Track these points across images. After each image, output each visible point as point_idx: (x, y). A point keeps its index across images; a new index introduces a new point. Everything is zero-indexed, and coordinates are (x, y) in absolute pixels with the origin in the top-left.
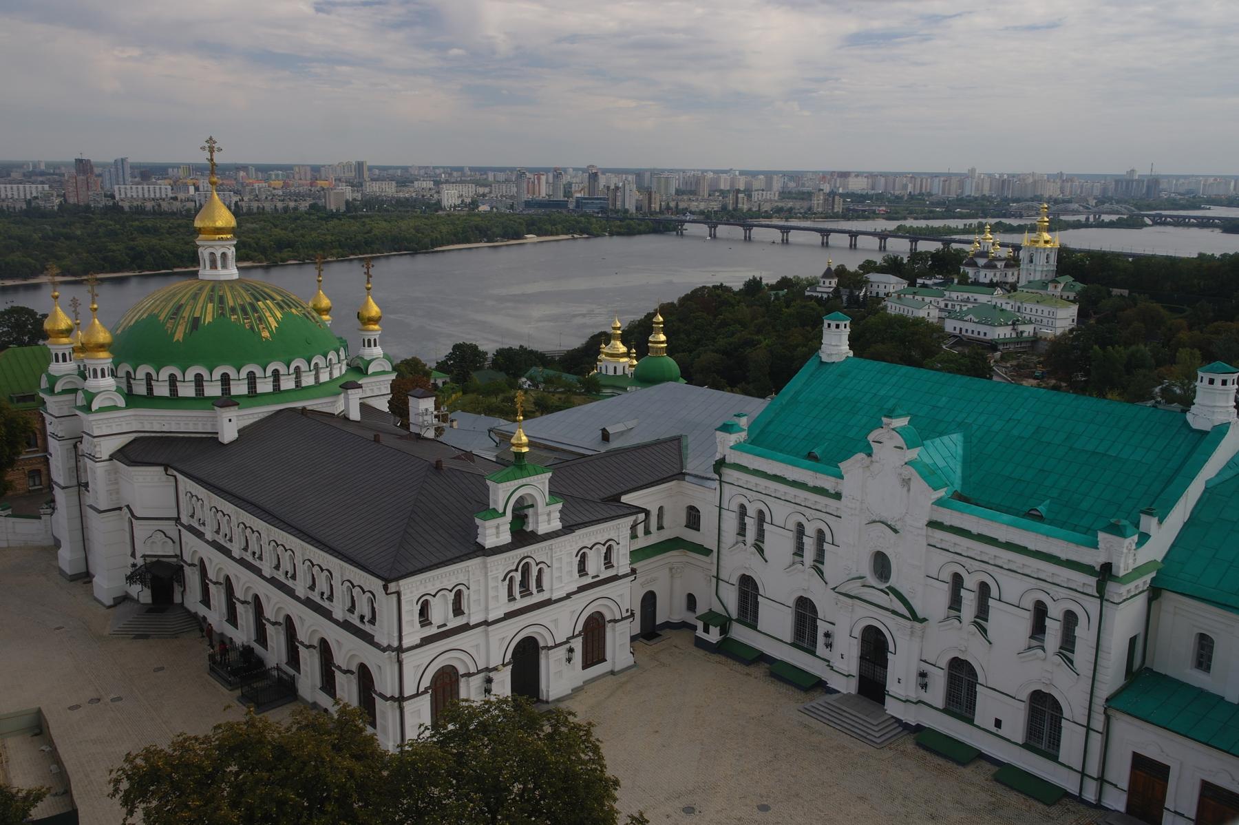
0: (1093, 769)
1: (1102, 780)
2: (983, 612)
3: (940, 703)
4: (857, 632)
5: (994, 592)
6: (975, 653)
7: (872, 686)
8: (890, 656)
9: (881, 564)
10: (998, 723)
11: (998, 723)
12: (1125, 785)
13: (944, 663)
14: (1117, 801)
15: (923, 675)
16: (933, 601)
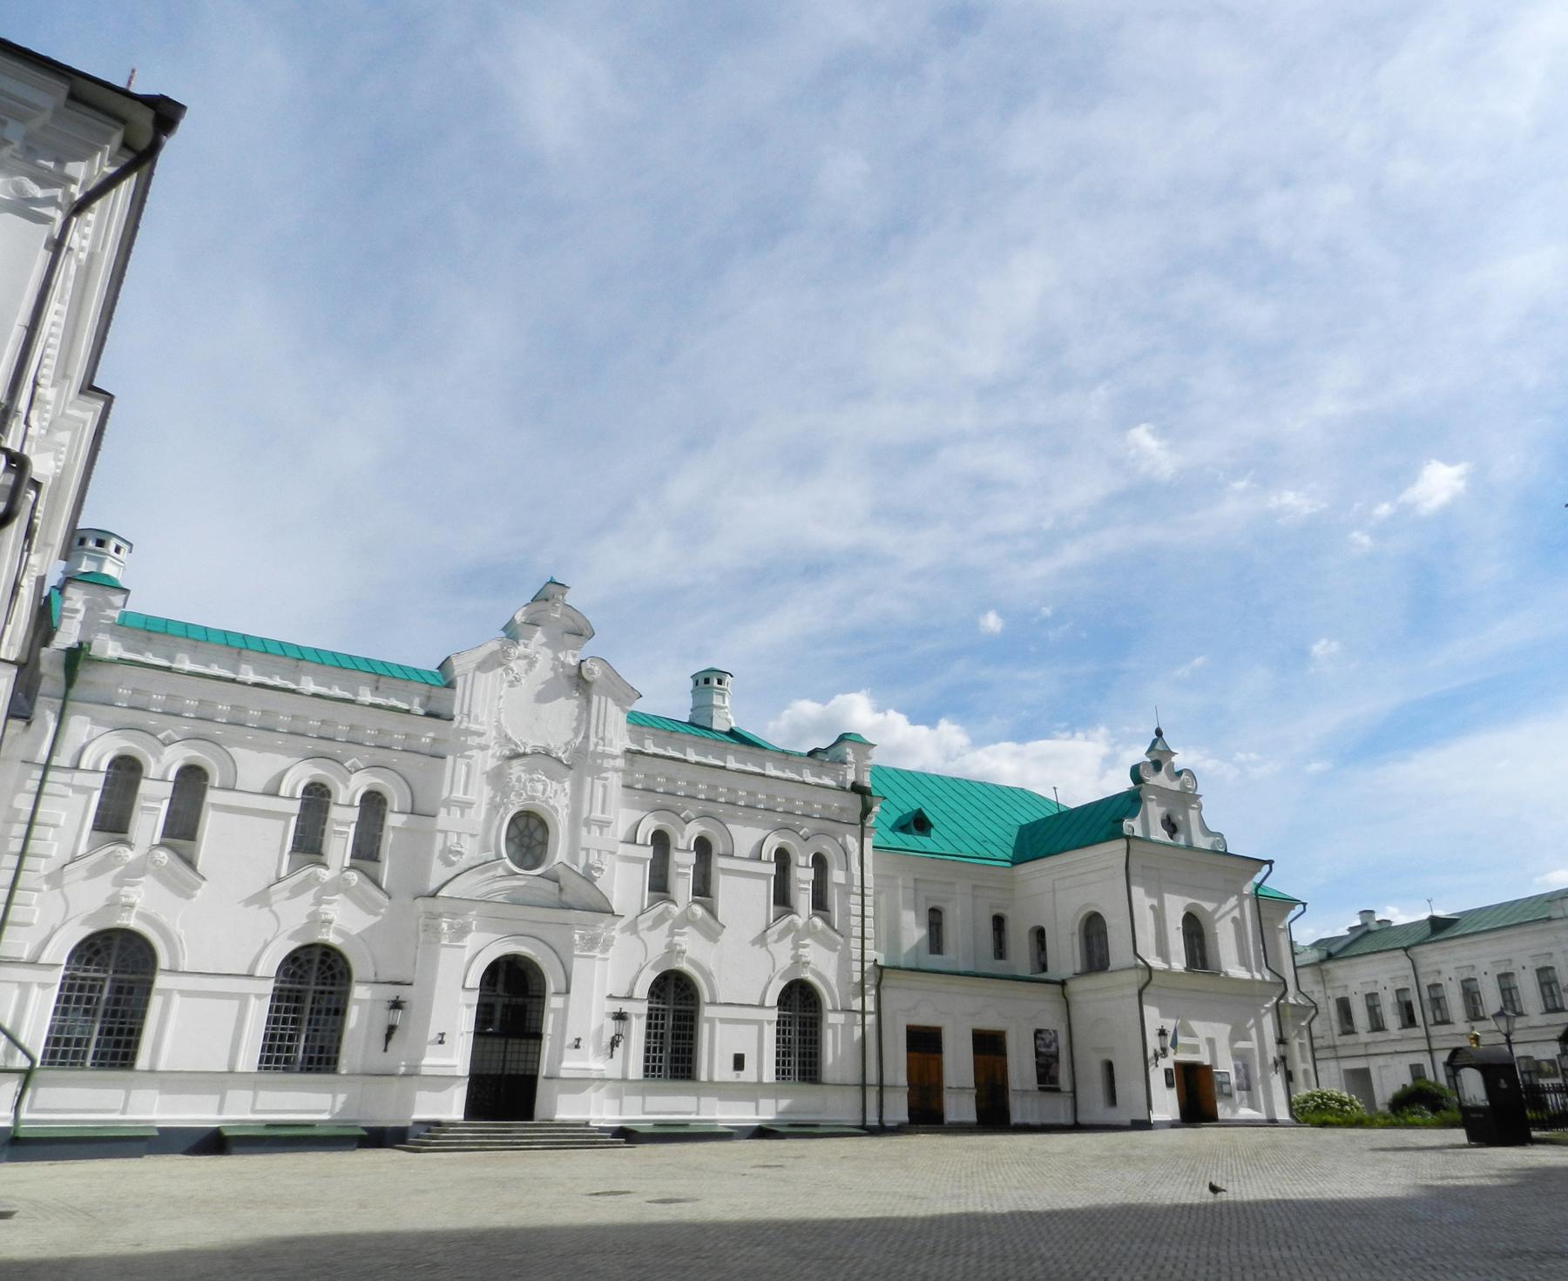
0: (872, 1077)
1: (881, 1085)
2: (703, 888)
3: (636, 1068)
4: (474, 979)
5: (718, 846)
6: (695, 954)
7: (504, 1094)
8: (553, 1003)
9: (529, 835)
10: (739, 1062)
11: (739, 1062)
12: (902, 1079)
13: (642, 990)
14: (898, 1110)
15: (620, 1017)
16: (624, 882)
